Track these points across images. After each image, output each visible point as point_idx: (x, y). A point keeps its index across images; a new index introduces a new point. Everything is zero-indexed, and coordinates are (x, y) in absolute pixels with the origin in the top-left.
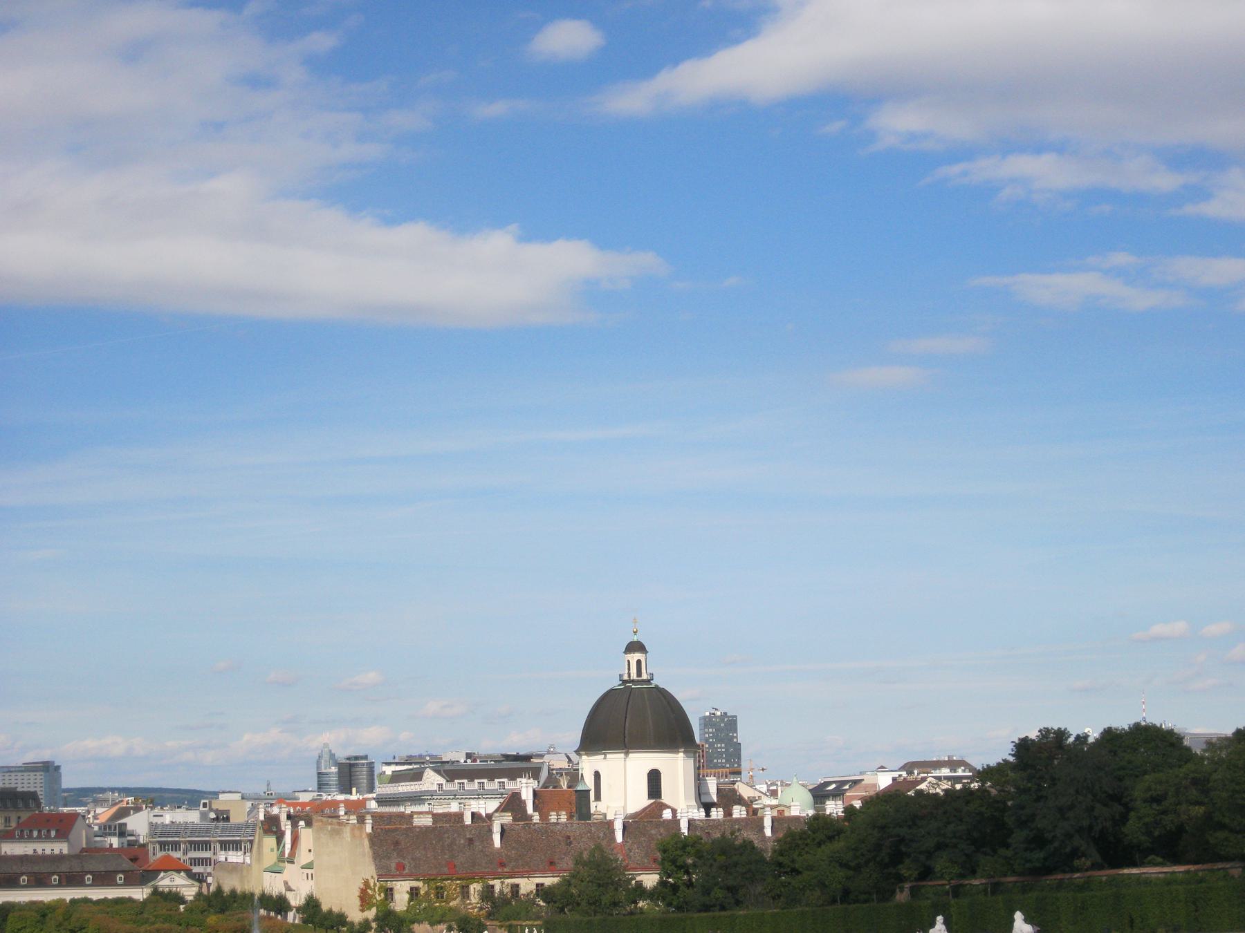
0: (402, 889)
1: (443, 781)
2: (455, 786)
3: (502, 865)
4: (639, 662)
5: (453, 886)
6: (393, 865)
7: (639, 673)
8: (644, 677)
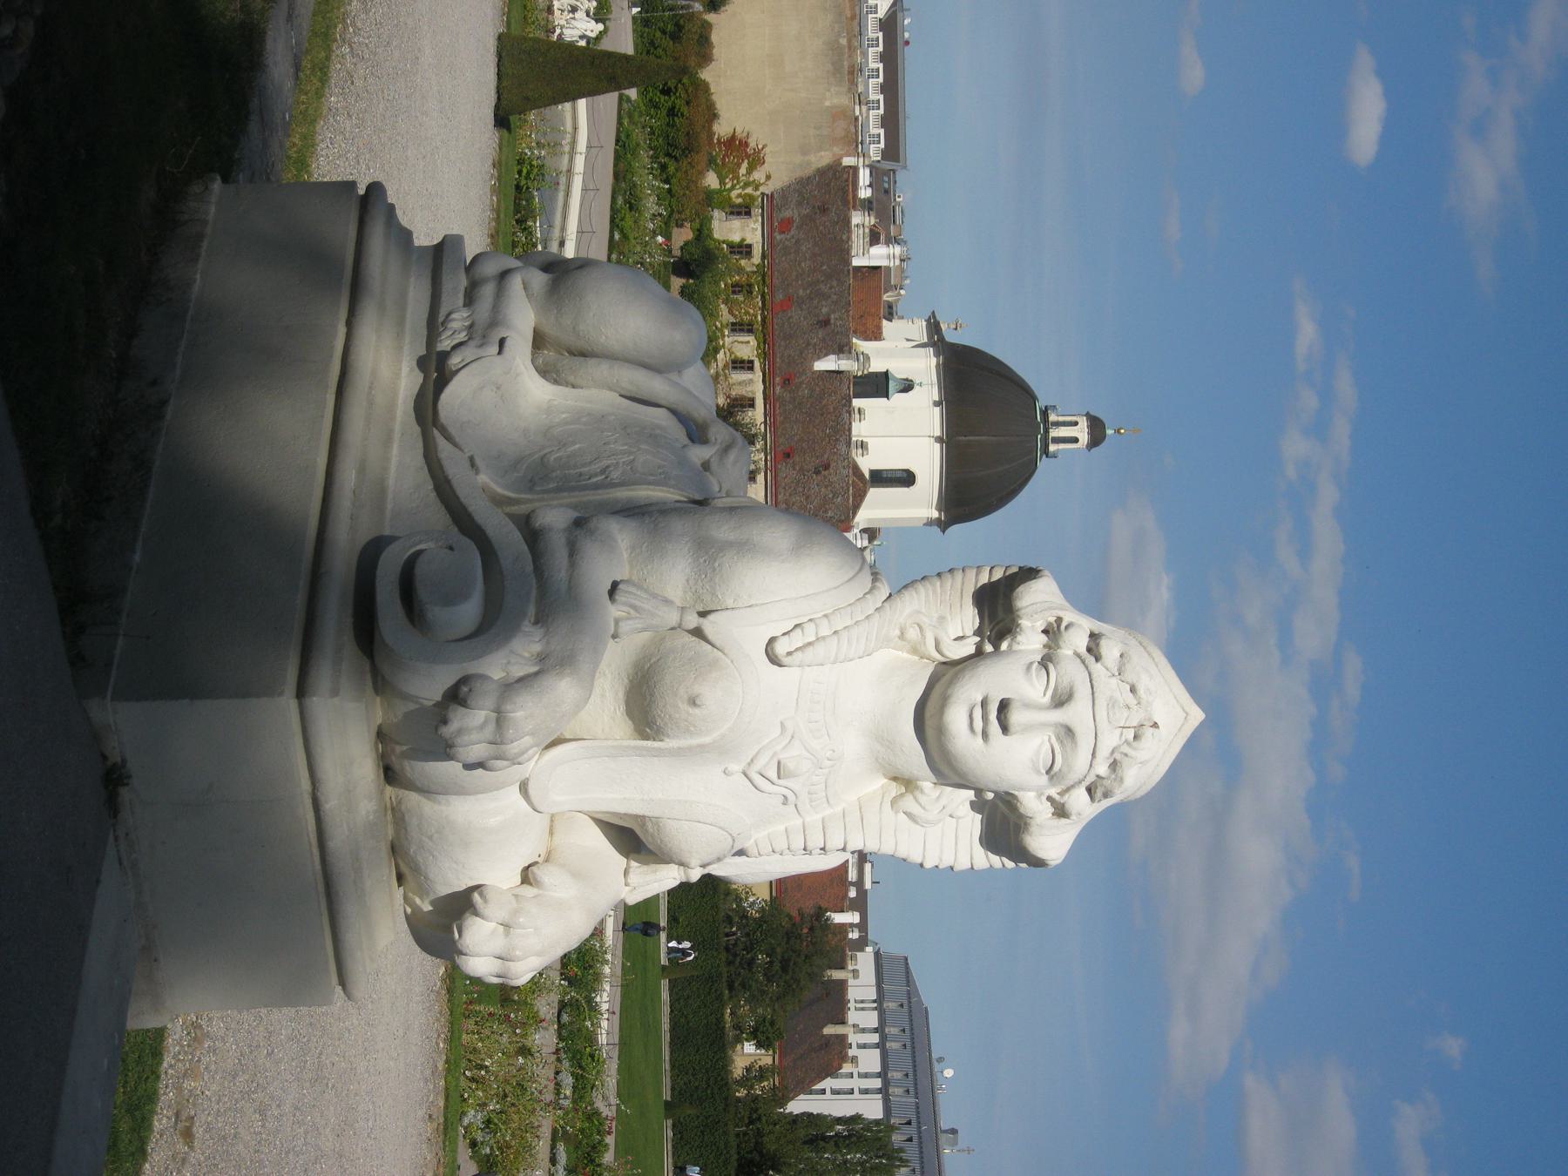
0: (749, 231)
1: (881, 13)
2: (873, 32)
3: (787, 382)
4: (1076, 440)
5: (753, 310)
6: (787, 214)
7: (1058, 440)
8: (1052, 448)
